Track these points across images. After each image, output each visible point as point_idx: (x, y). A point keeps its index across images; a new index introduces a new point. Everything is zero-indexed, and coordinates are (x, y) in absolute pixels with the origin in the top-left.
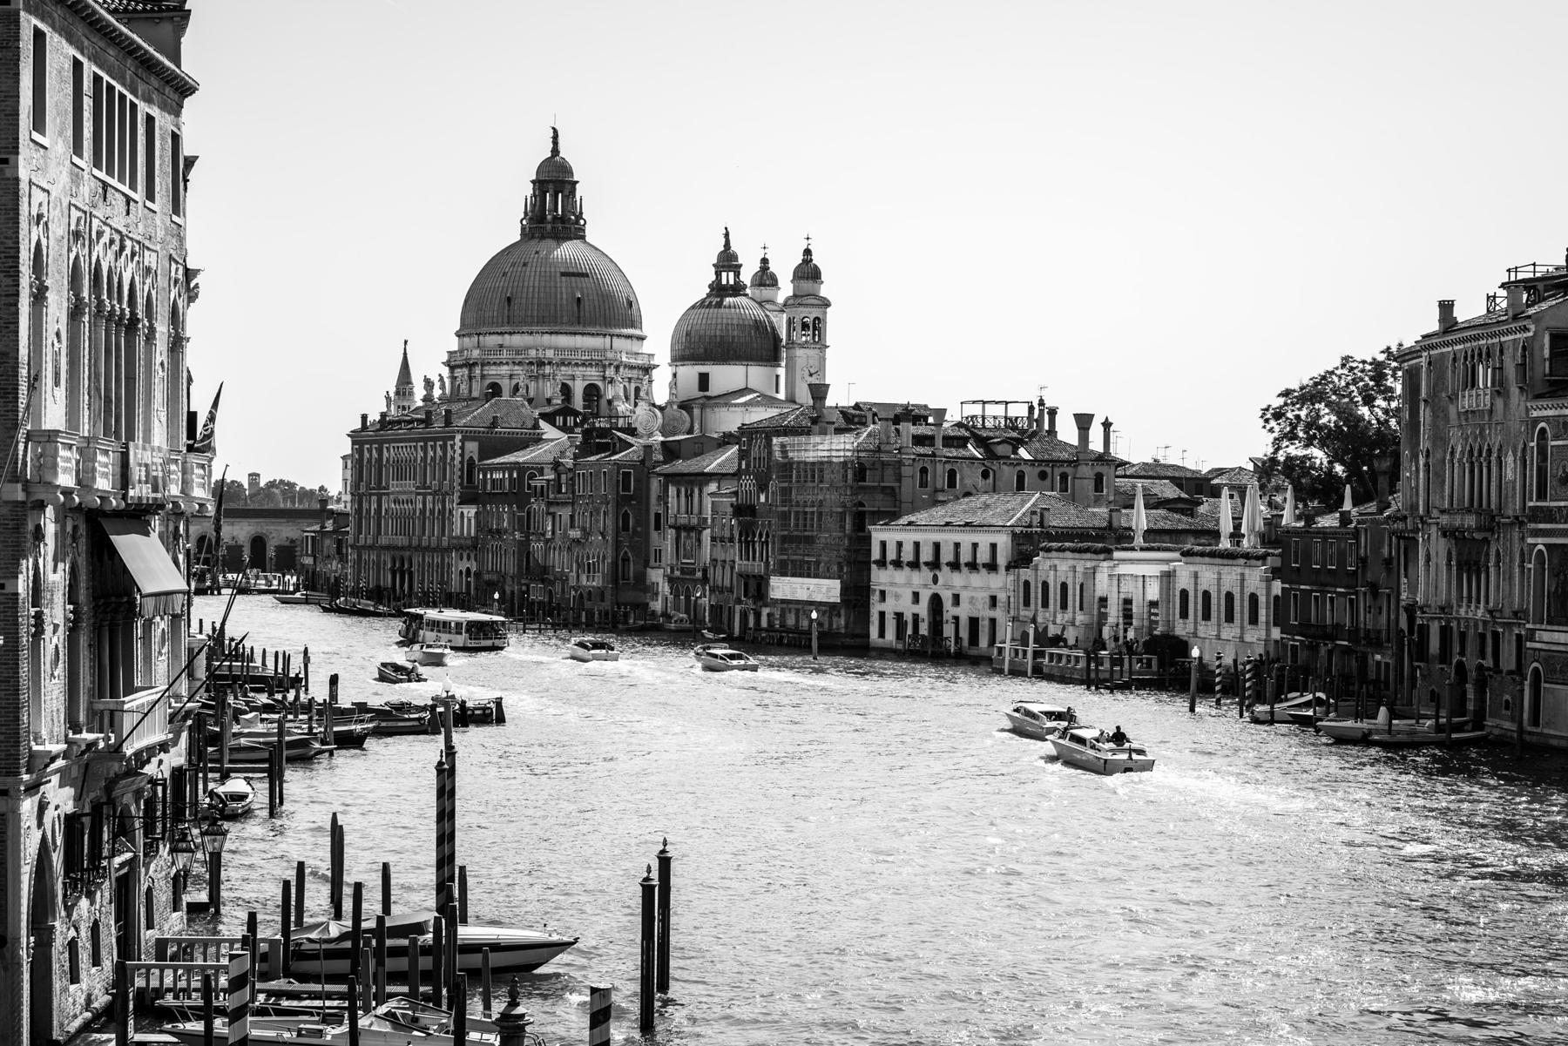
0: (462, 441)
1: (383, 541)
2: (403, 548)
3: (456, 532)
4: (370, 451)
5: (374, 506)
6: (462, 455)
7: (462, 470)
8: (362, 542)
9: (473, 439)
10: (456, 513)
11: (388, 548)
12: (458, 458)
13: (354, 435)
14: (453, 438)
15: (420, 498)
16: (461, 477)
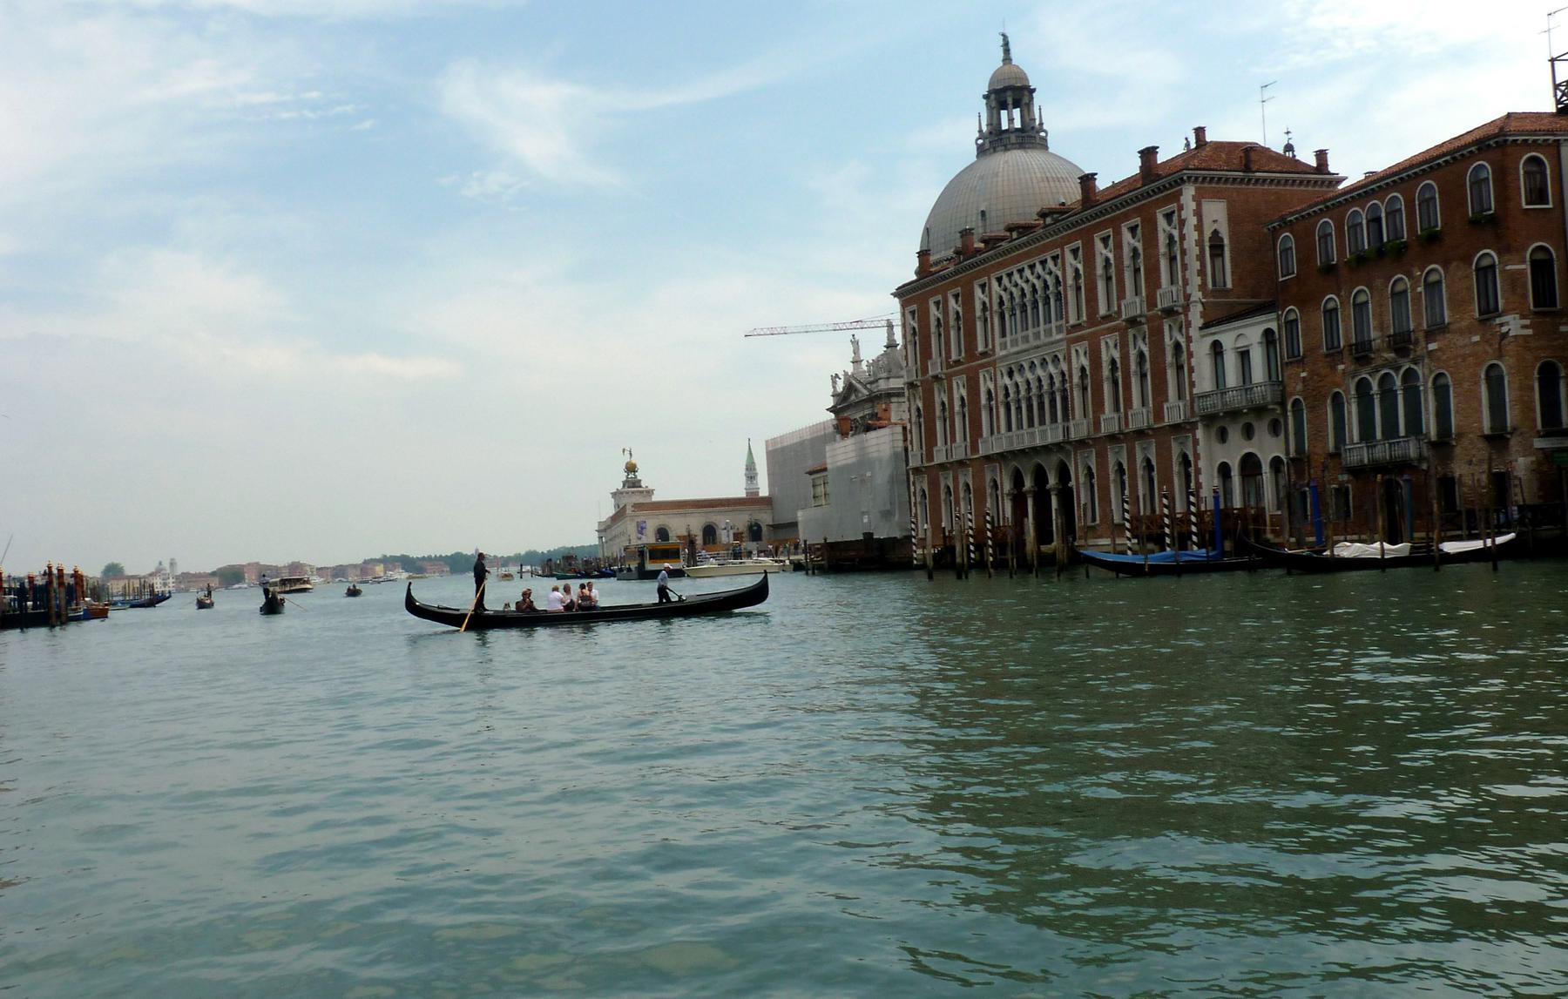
0: (1198, 199)
1: (991, 445)
2: (1047, 449)
3: (1204, 381)
4: (943, 305)
5: (960, 391)
6: (1199, 228)
7: (1201, 257)
8: (939, 458)
9: (1217, 195)
10: (1201, 349)
11: (1002, 457)
12: (1192, 236)
13: (903, 293)
14: (1176, 197)
15: (1082, 347)
16: (1202, 273)
